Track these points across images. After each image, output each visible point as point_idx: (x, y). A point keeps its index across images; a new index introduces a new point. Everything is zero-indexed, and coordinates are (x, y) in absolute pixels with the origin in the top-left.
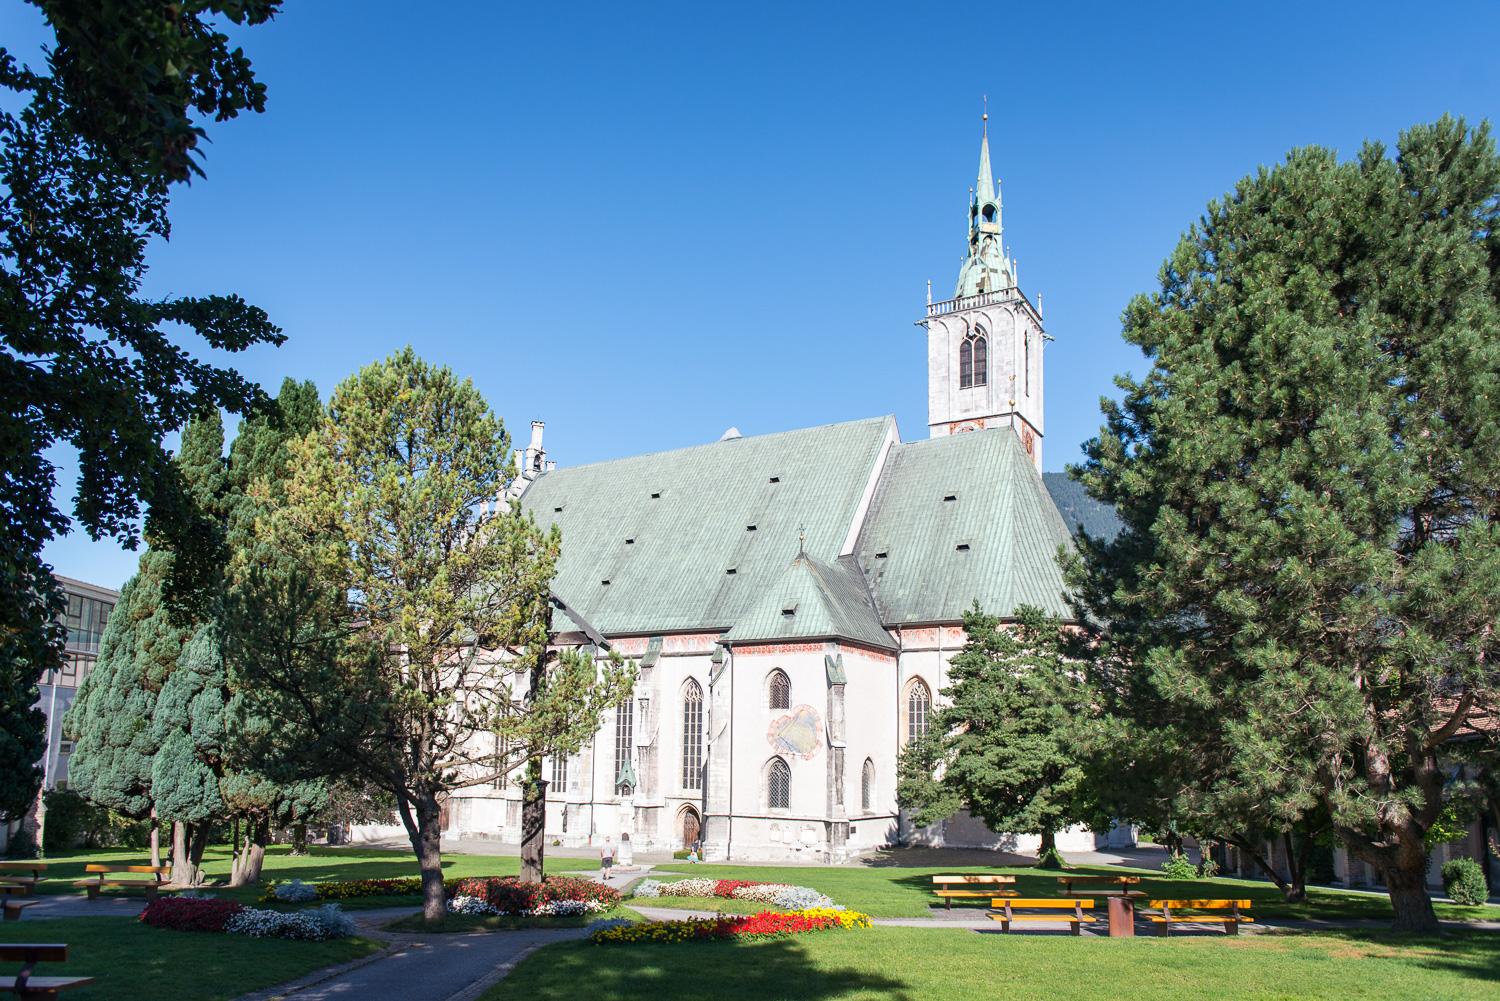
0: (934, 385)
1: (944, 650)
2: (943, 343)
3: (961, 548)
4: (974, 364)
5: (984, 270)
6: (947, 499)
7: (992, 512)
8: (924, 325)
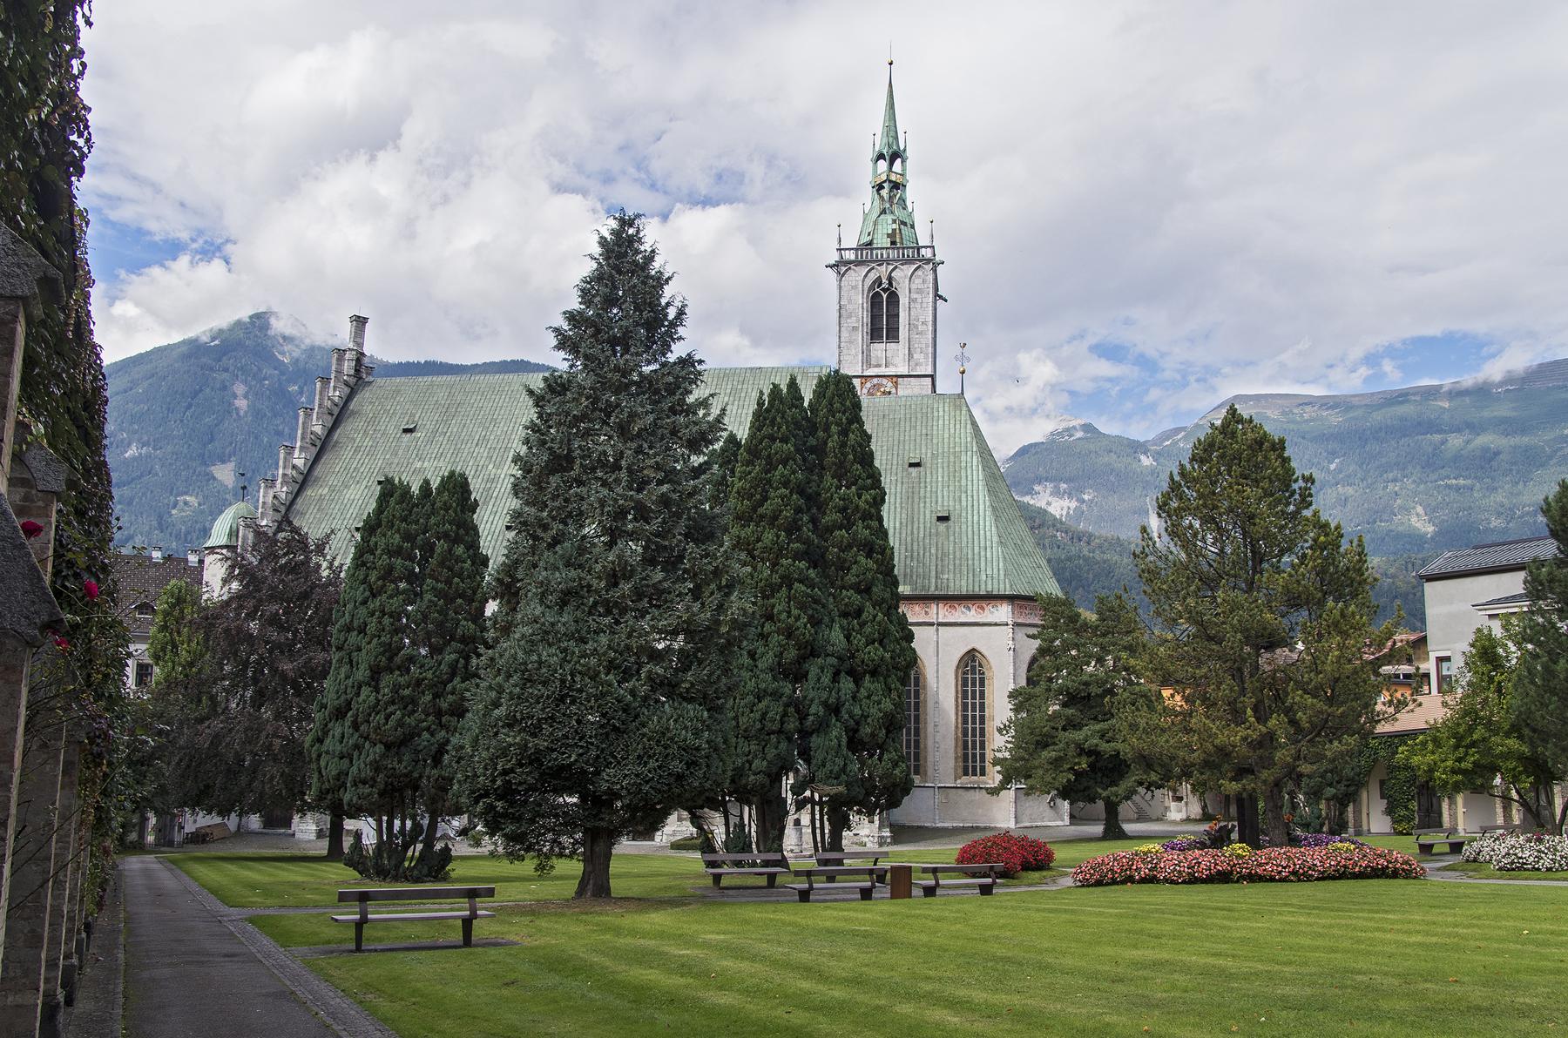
1: (932, 624)
3: (940, 519)
6: (911, 465)
7: (963, 482)
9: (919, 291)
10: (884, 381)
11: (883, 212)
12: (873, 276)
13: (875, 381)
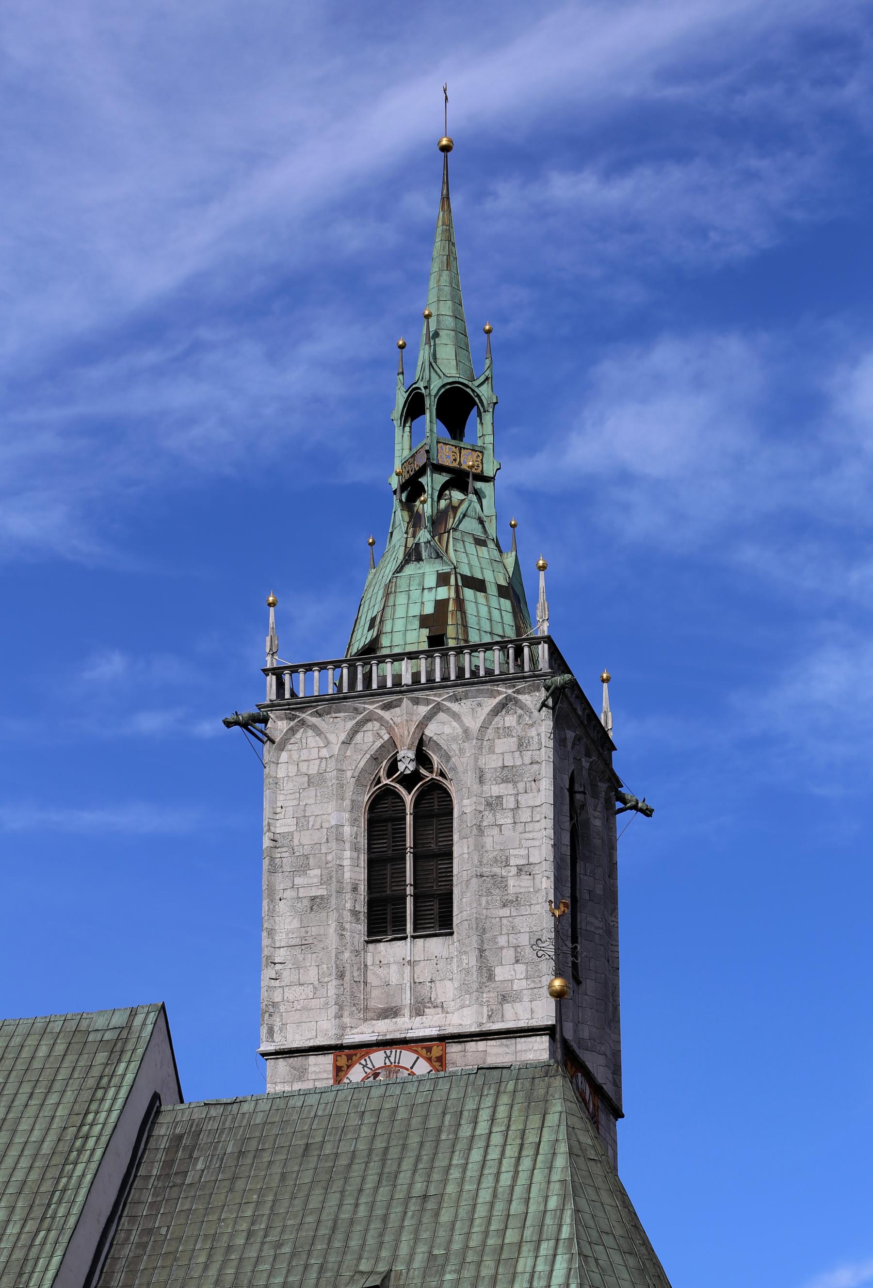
0: (284, 923)
2: (312, 793)
4: (407, 869)
5: (443, 580)
8: (253, 724)
9: (508, 775)
10: (407, 1057)
11: (413, 555)
12: (370, 739)
13: (378, 1058)
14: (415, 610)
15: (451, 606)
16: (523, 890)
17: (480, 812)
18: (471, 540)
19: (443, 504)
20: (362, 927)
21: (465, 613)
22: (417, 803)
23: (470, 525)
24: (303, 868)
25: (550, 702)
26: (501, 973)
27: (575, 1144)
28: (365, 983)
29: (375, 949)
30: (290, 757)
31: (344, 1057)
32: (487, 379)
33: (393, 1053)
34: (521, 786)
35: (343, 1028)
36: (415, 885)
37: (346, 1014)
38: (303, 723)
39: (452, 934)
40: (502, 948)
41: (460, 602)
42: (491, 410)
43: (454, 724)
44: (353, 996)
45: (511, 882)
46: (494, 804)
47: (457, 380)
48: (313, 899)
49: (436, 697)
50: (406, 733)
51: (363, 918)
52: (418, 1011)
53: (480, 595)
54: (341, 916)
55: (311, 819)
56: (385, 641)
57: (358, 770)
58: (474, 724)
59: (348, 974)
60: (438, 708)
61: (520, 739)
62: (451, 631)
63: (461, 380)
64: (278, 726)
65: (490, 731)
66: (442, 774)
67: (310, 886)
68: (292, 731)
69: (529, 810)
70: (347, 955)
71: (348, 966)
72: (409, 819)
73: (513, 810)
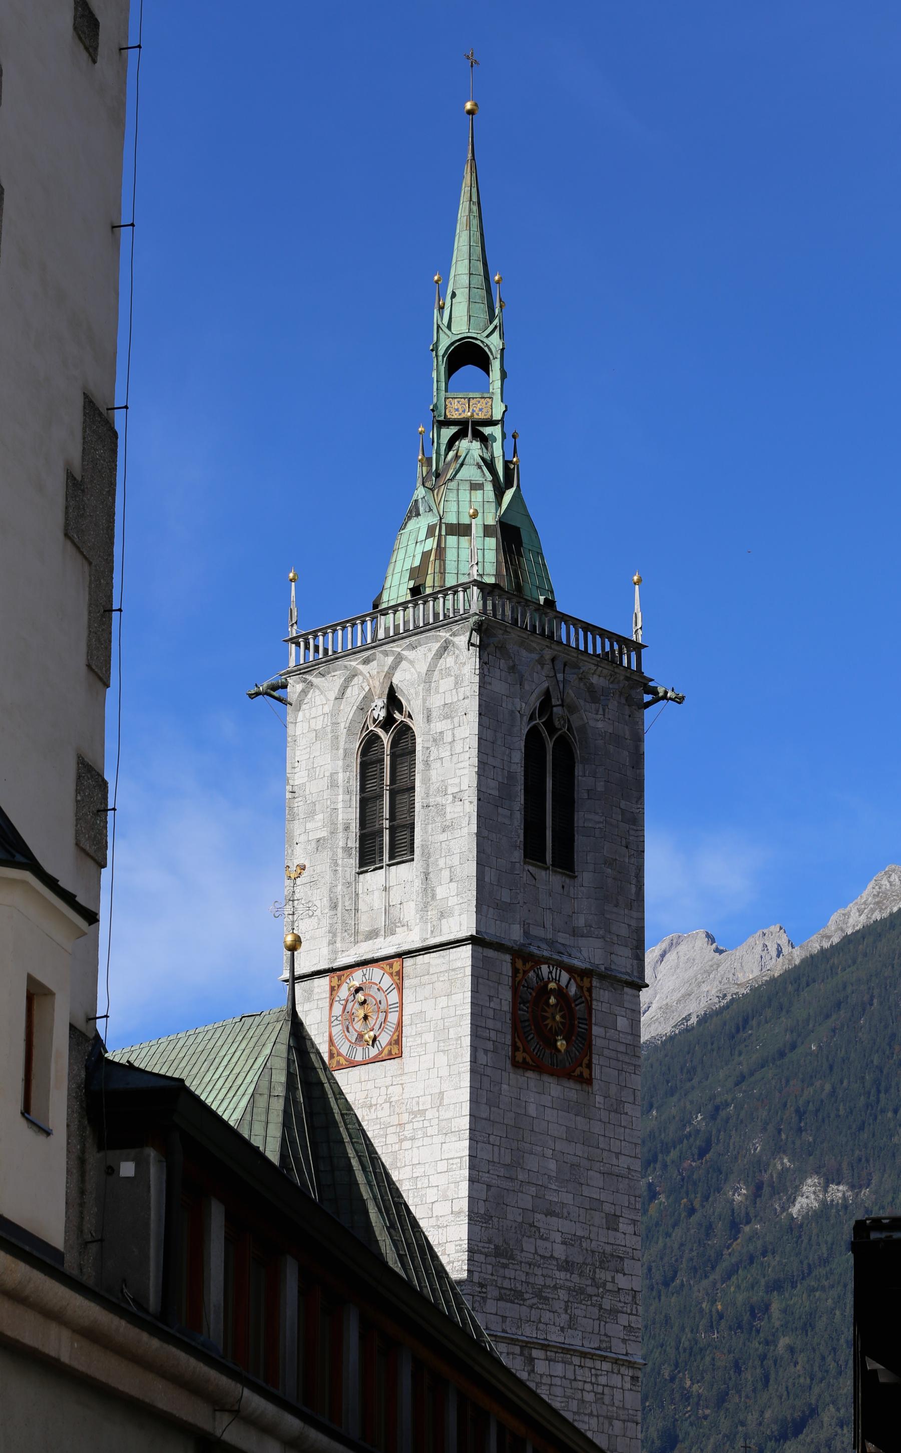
9: (448, 712)
12: (355, 694)
14: (407, 566)
15: (432, 558)
16: (456, 815)
17: (428, 748)
18: (468, 487)
19: (451, 454)
20: (354, 861)
21: (444, 561)
22: (394, 744)
23: (470, 472)
24: (311, 814)
25: (476, 639)
26: (440, 892)
27: (264, 1083)
28: (357, 910)
29: (364, 878)
30: (304, 716)
31: (336, 978)
32: (496, 327)
33: (367, 970)
34: (456, 720)
35: (335, 952)
36: (392, 818)
37: (338, 939)
38: (311, 684)
39: (413, 860)
40: (441, 870)
41: (441, 551)
42: (499, 356)
43: (412, 670)
44: (344, 922)
45: (448, 809)
46: (438, 740)
47: (466, 335)
48: (318, 841)
49: (396, 648)
50: (378, 683)
51: (355, 854)
52: (390, 930)
53: (464, 540)
54: (335, 854)
55: (318, 769)
56: (385, 597)
57: (349, 721)
58: (423, 667)
59: (340, 904)
60: (399, 659)
61: (456, 677)
62: (429, 581)
63: (469, 335)
64: (295, 688)
65: (436, 673)
66: (410, 716)
67: (316, 829)
68: (304, 692)
69: (462, 741)
70: (340, 887)
71: (340, 897)
72: (387, 760)
73: (450, 743)
